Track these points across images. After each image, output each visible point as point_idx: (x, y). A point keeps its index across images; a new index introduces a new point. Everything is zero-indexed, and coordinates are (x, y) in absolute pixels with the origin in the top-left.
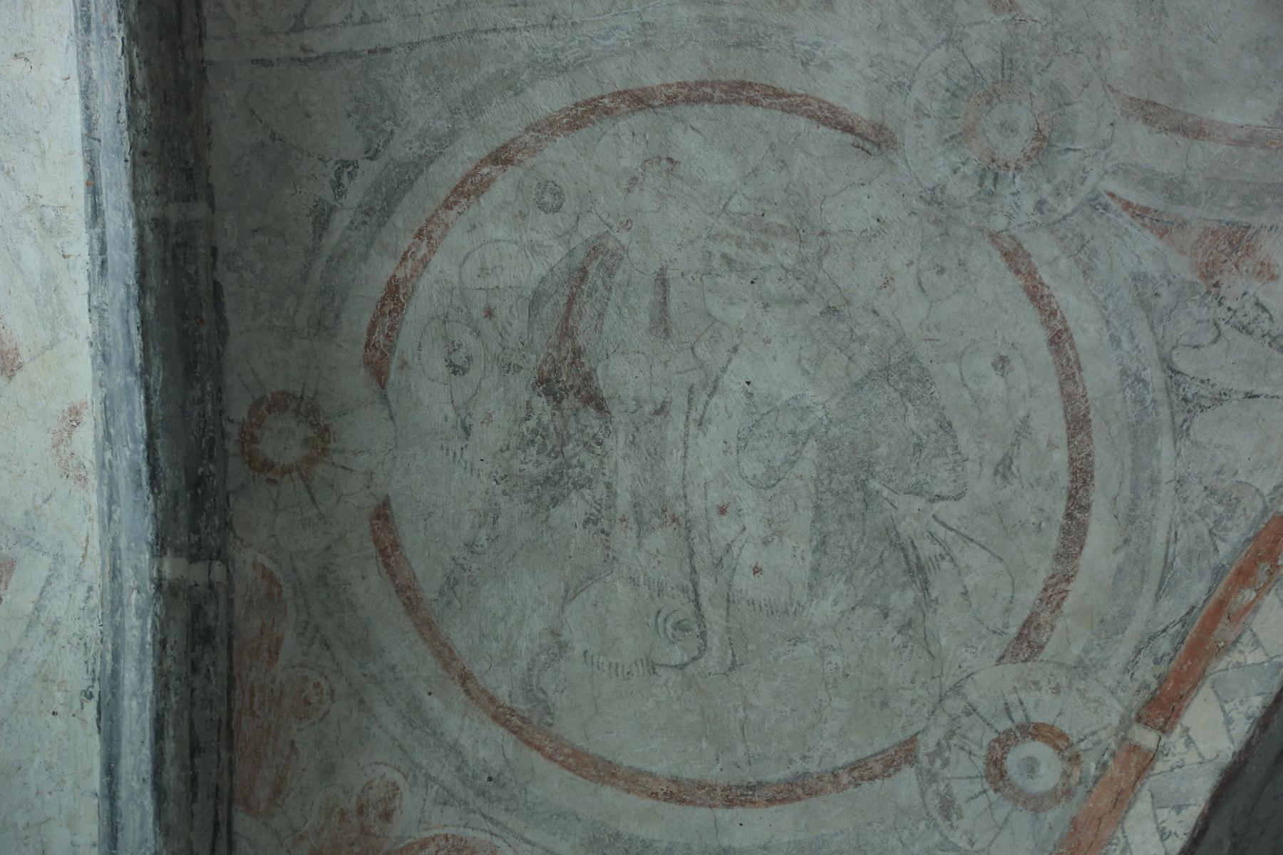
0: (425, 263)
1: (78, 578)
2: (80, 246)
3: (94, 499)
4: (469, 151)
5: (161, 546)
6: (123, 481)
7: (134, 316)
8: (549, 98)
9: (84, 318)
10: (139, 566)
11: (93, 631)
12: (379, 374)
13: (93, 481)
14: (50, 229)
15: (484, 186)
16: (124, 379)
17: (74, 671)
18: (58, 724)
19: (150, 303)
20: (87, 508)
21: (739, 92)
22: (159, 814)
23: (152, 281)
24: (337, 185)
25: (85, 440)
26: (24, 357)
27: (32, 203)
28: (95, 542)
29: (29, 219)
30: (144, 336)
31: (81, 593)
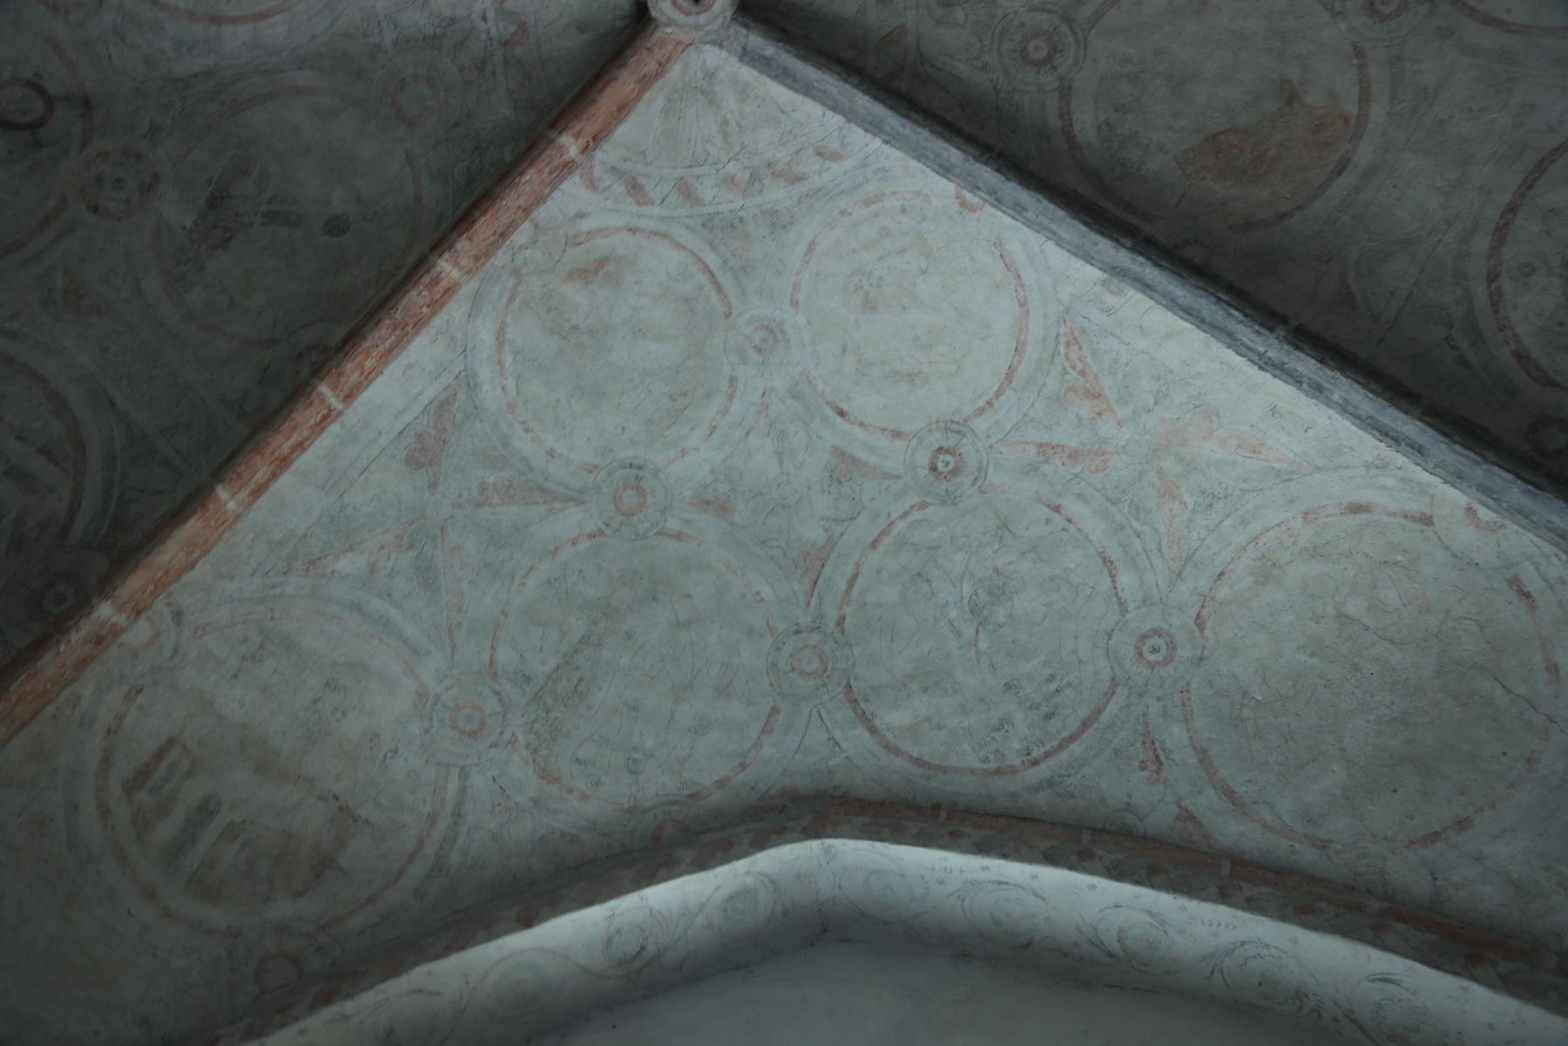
0: (1515, 335)
1: (1547, 557)
2: (1400, 459)
3: (1515, 527)
4: (1480, 290)
6: (1527, 503)
8: (1481, 244)
9: (1433, 478)
12: (1552, 384)
13: (1507, 522)
14: (1383, 466)
15: (1500, 292)
16: (1479, 472)
20: (1517, 533)
21: (1542, 167)
24: (1453, 347)
25: (1484, 513)
26: (1428, 512)
27: (1368, 466)
28: (1536, 539)
29: (1373, 471)
30: (1470, 449)
31: (1555, 560)
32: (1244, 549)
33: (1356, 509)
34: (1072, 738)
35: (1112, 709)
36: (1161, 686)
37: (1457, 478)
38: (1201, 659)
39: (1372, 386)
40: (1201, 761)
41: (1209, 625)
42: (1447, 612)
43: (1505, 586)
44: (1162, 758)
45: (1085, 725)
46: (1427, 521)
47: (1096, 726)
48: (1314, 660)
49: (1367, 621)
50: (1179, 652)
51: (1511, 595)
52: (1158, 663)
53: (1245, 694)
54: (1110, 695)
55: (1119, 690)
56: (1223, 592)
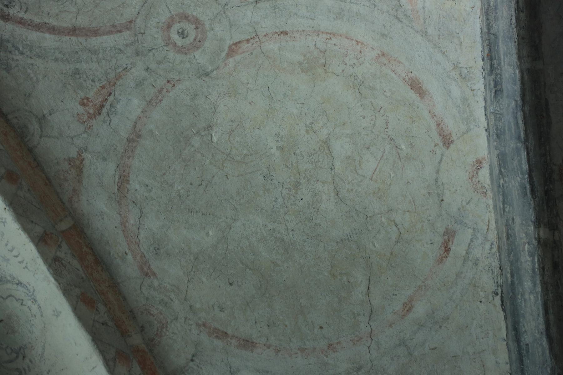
1: (486, 239)
2: (479, 85)
3: (491, 202)
5: (538, 223)
7: (520, 115)
9: (483, 119)
10: (526, 233)
11: (496, 264)
13: (490, 194)
14: (465, 77)
17: (488, 282)
18: (483, 307)
19: (527, 108)
20: (488, 207)
22: (551, 349)
23: (528, 98)
25: (484, 175)
26: (454, 137)
27: (456, 67)
28: (493, 222)
29: (455, 74)
30: (525, 124)
31: (487, 246)
32: (318, 33)
33: (416, 86)
34: (53, 30)
35: (109, 41)
36: (159, 63)
37: (496, 134)
38: (207, 74)
39: (523, 16)
40: (129, 140)
41: (238, 57)
42: (390, 210)
43: (442, 230)
44: (105, 110)
45: (74, 31)
46: (447, 141)
47: (81, 39)
48: (278, 153)
49: (338, 164)
50: (197, 54)
51: (438, 240)
52: (175, 45)
53: (209, 127)
54: (116, 29)
55: (126, 34)
56: (272, 46)
